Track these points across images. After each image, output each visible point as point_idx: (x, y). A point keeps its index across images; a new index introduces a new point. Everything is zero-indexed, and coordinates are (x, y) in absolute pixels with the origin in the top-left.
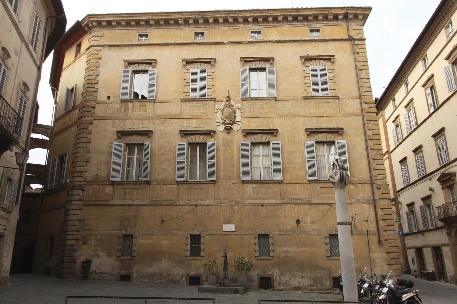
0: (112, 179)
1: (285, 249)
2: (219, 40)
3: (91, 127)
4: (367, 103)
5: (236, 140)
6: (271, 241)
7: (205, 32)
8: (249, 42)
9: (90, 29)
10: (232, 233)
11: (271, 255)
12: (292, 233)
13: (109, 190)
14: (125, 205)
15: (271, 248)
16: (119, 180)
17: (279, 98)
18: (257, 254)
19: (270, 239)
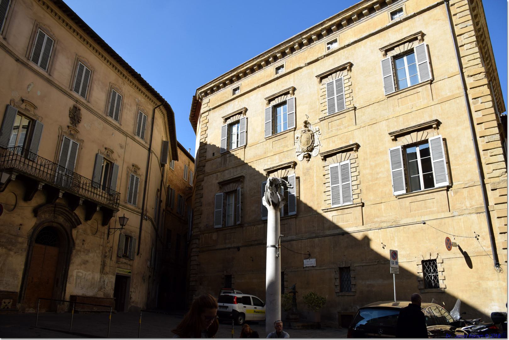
0: (216, 227)
1: (368, 283)
2: (298, 66)
3: (203, 183)
4: (471, 76)
5: (315, 166)
6: (352, 274)
7: (284, 63)
8: (325, 56)
9: (202, 100)
10: (313, 268)
11: (353, 290)
12: (376, 263)
13: (214, 236)
14: (226, 248)
15: (353, 282)
16: (220, 226)
17: (357, 106)
18: (338, 289)
19: (351, 272)
